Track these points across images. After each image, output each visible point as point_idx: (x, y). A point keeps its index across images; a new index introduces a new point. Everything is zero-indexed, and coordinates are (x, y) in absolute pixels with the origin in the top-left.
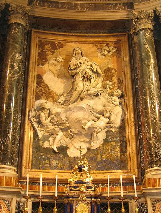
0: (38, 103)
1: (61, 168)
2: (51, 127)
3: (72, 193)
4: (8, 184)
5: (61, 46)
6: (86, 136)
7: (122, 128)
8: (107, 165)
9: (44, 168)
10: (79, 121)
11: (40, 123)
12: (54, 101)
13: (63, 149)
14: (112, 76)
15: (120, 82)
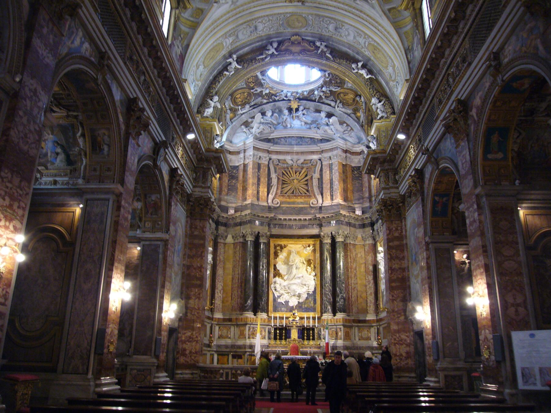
0: (274, 280)
1: (287, 312)
2: (282, 292)
3: (290, 325)
4: (264, 321)
5: (285, 246)
6: (298, 296)
7: (314, 292)
8: (307, 310)
9: (278, 311)
10: (294, 290)
11: (275, 290)
12: (282, 278)
13: (287, 302)
14: (311, 264)
15: (315, 267)
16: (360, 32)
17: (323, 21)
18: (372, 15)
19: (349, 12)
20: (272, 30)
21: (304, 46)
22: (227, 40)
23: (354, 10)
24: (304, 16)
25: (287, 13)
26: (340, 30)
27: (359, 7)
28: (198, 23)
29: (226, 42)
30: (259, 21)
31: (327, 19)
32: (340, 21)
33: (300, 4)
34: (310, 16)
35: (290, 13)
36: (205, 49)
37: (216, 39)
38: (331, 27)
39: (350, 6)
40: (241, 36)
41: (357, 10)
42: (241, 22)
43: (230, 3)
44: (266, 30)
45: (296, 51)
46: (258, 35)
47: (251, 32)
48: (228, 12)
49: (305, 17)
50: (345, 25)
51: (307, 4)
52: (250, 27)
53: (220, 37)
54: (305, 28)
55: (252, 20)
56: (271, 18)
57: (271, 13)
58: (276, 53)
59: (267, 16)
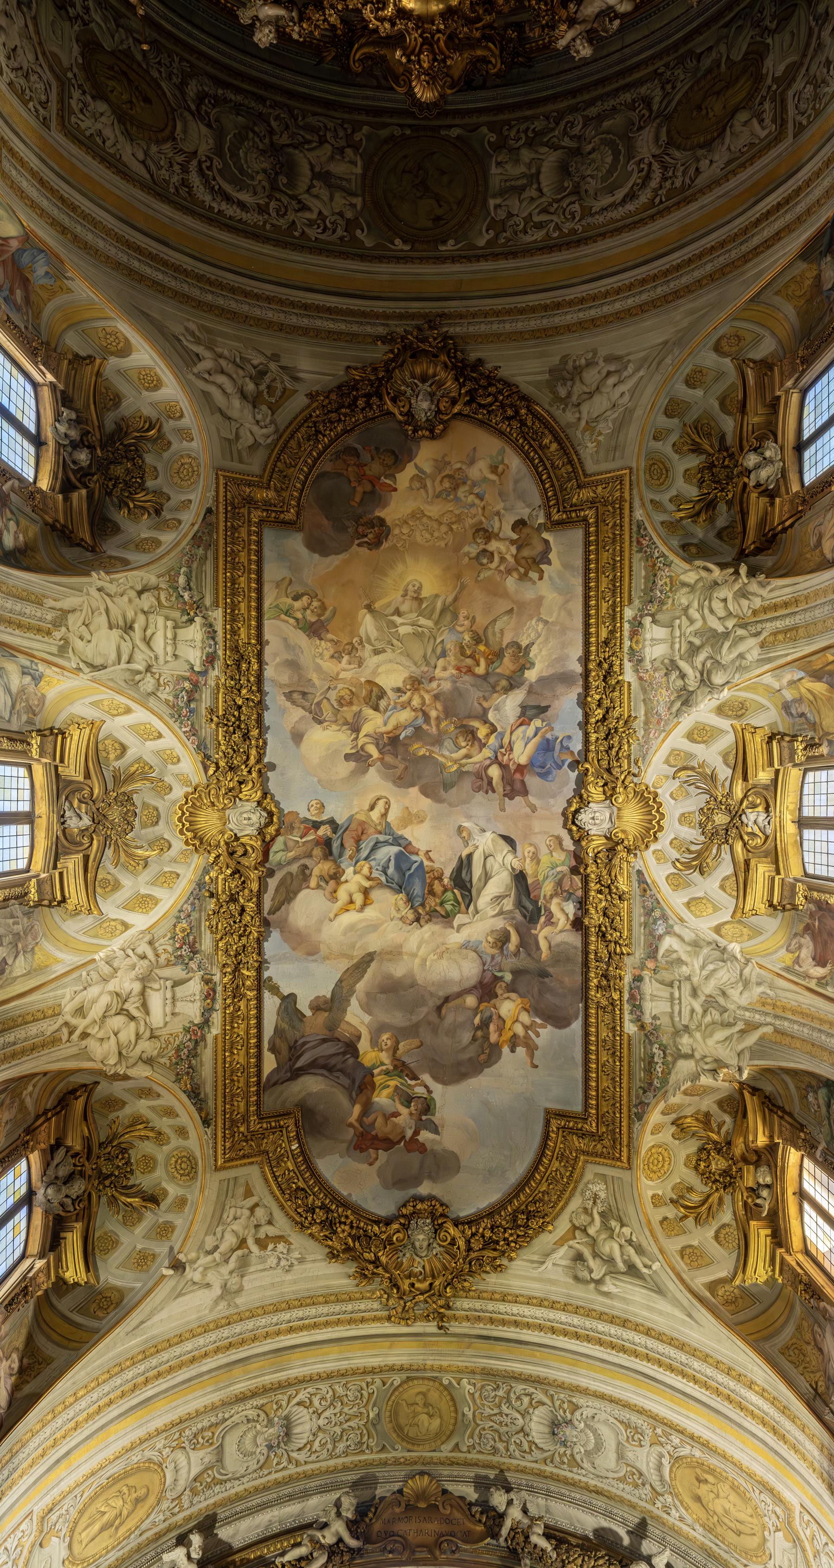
16: (635, 1419)
17: (508, 1401)
18: (660, 1323)
19: (588, 1339)
20: (341, 1446)
21: (448, 1520)
22: (181, 1457)
23: (601, 1327)
24: (445, 1382)
25: (392, 1369)
26: (568, 1431)
27: (617, 1307)
28: (97, 1331)
29: (176, 1470)
30: (302, 1396)
31: (519, 1387)
32: (562, 1386)
33: (431, 1327)
34: (465, 1381)
35: (402, 1369)
36: (93, 1464)
37: (141, 1433)
38: (537, 1425)
39: (588, 1313)
40: (233, 1462)
41: (613, 1320)
42: (240, 1387)
43: (217, 1291)
44: (323, 1445)
45: (420, 1539)
46: (292, 1470)
47: (270, 1447)
48: (205, 1329)
49: (448, 1388)
50: (581, 1401)
51: (455, 1328)
52: (270, 1423)
53: (158, 1432)
54: (448, 1446)
55: (280, 1386)
56: (340, 1391)
57: (343, 1365)
58: (353, 1543)
59: (329, 1376)
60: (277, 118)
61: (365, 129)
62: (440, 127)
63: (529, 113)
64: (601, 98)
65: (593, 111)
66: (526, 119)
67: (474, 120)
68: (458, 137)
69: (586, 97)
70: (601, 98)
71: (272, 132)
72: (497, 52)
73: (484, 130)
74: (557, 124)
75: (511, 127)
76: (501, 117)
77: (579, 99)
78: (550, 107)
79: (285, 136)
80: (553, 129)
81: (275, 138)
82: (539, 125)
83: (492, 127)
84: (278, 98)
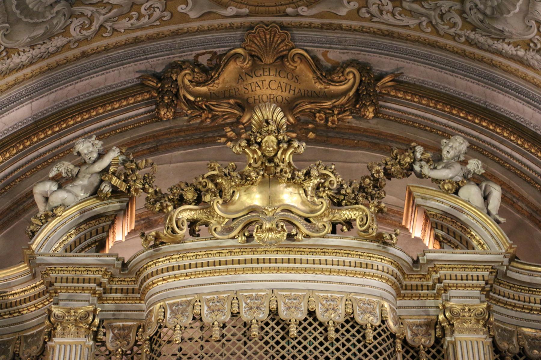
60: (455, 25)
61: (343, 12)
62: (247, 16)
63: (139, 33)
64: (51, 55)
65: (59, 41)
66: (141, 28)
67: (206, 23)
68: (226, 6)
69: (70, 54)
70: (51, 55)
71: (462, 13)
72: (182, 92)
73: (193, 15)
74: (101, 26)
75: (160, 18)
76: (173, 28)
77: (77, 52)
78: (113, 41)
79: (445, 9)
80: (106, 21)
81: (458, 6)
82: (125, 23)
83: (184, 17)
84: (450, 43)
